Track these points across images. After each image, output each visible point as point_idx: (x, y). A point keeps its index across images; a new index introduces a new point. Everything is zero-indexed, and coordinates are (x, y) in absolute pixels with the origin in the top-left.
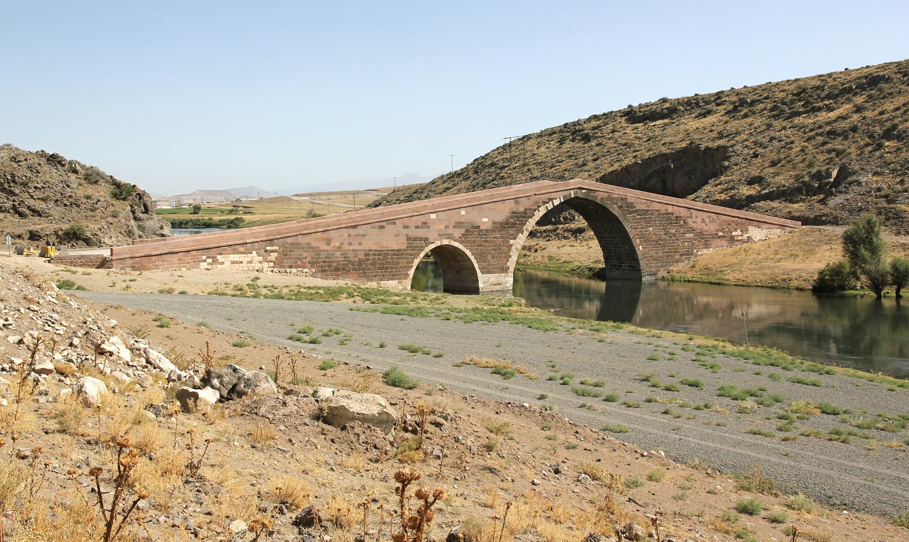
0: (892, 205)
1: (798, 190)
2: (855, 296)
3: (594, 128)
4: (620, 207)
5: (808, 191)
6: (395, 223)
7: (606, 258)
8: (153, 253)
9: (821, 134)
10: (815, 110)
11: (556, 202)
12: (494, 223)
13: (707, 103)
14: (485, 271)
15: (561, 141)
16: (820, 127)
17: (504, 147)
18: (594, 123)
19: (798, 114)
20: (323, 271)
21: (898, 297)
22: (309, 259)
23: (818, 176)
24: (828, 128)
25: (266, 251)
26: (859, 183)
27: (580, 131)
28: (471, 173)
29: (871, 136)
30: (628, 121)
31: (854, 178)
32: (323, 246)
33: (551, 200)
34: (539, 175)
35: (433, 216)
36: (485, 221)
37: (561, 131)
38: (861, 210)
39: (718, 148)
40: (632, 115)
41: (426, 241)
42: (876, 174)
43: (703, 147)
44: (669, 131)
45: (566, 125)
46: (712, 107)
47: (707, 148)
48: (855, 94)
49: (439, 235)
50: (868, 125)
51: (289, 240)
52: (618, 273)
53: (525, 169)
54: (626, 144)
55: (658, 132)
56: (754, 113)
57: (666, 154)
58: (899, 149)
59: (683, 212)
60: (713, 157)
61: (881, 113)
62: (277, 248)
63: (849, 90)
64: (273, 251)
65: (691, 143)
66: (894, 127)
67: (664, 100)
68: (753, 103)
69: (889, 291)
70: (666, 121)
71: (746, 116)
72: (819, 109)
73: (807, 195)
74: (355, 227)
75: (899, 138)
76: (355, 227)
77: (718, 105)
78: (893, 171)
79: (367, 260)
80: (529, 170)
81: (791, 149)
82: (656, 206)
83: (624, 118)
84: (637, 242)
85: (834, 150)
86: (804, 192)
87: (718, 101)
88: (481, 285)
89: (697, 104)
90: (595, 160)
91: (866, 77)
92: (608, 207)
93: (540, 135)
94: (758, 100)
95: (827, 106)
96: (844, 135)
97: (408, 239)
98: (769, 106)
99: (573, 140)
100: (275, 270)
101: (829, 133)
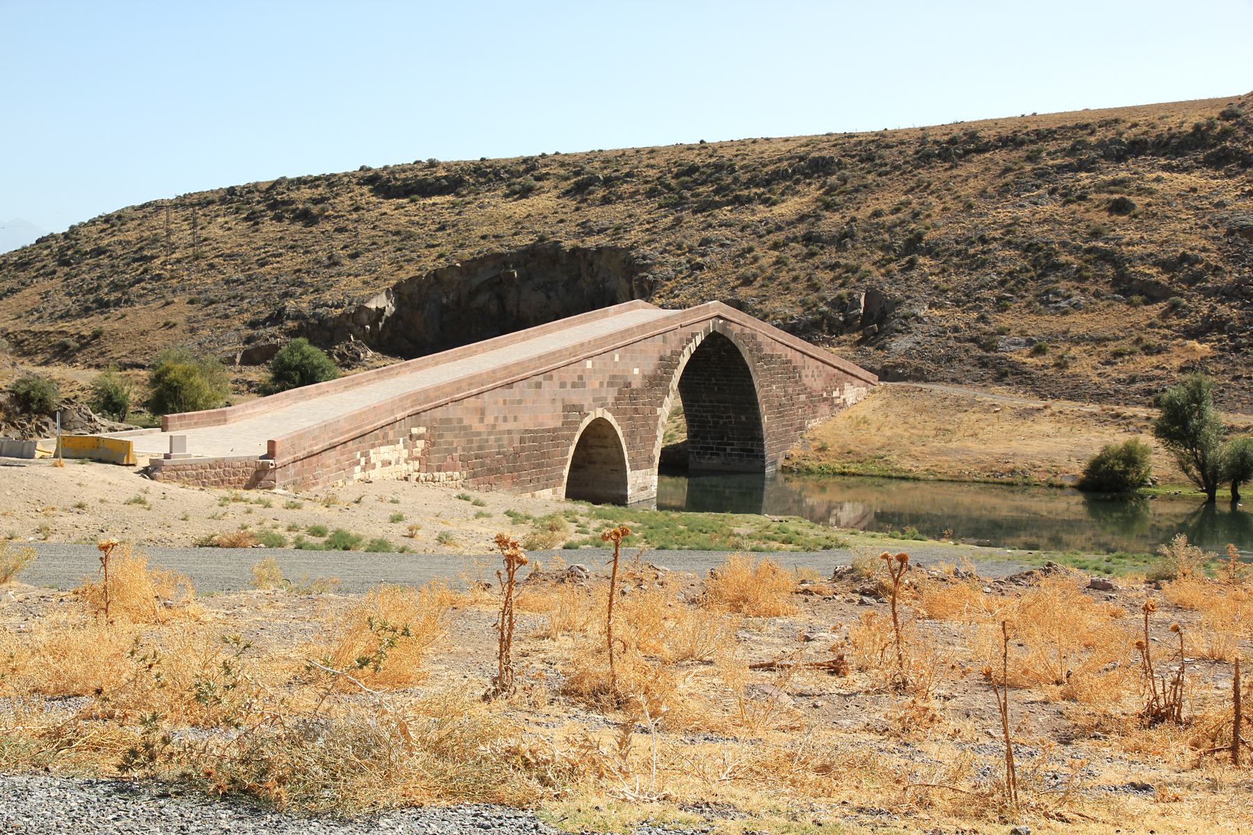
0: (992, 354)
1: (816, 325)
2: (1143, 497)
3: (316, 202)
4: (751, 351)
5: (830, 326)
6: (551, 378)
7: (693, 434)
8: (316, 449)
9: (795, 239)
10: (739, 201)
11: (698, 340)
12: (644, 377)
13: (513, 174)
14: (633, 468)
15: (254, 218)
16: (779, 228)
17: (107, 219)
18: (306, 193)
19: (718, 205)
20: (474, 476)
21: (1236, 498)
22: (460, 452)
23: (839, 304)
24: (801, 229)
25: (411, 436)
26: (919, 320)
27: (284, 203)
28: (52, 264)
29: (886, 248)
30: (376, 191)
31: (905, 310)
32: (477, 426)
33: (694, 335)
34: (241, 276)
35: (589, 364)
36: (636, 373)
37: (223, 201)
38: (950, 360)
39: (599, 250)
40: (382, 184)
41: (580, 410)
42: (932, 305)
43: (568, 244)
44: (471, 213)
45: (231, 191)
46: (529, 180)
47: (575, 250)
48: (797, 182)
49: (594, 400)
50: (865, 231)
51: (438, 413)
52: (715, 461)
53: (203, 264)
54: (398, 233)
55: (449, 217)
56: (620, 197)
57: (501, 255)
58: (944, 270)
59: (798, 359)
60: (591, 264)
61: (877, 214)
62: (422, 430)
63: (779, 176)
64: (419, 437)
65: (542, 239)
66: (919, 237)
67: (432, 164)
68: (608, 182)
69: (1223, 492)
70: (450, 198)
71: (606, 201)
72: (750, 200)
73: (831, 333)
74: (509, 385)
75: (931, 252)
76: (509, 385)
77: (538, 179)
78: (957, 303)
79: (523, 450)
80: (212, 266)
81: (756, 259)
82: (780, 350)
83: (366, 189)
84: (763, 408)
85: (837, 265)
86: (825, 328)
87: (536, 173)
88: (629, 492)
89: (497, 174)
90: (354, 256)
91: (802, 159)
92: (741, 349)
93: (182, 203)
94: (617, 178)
95: (759, 196)
96: (841, 240)
97: (565, 408)
98: (643, 188)
99: (279, 218)
100: (422, 475)
101: (808, 239)
